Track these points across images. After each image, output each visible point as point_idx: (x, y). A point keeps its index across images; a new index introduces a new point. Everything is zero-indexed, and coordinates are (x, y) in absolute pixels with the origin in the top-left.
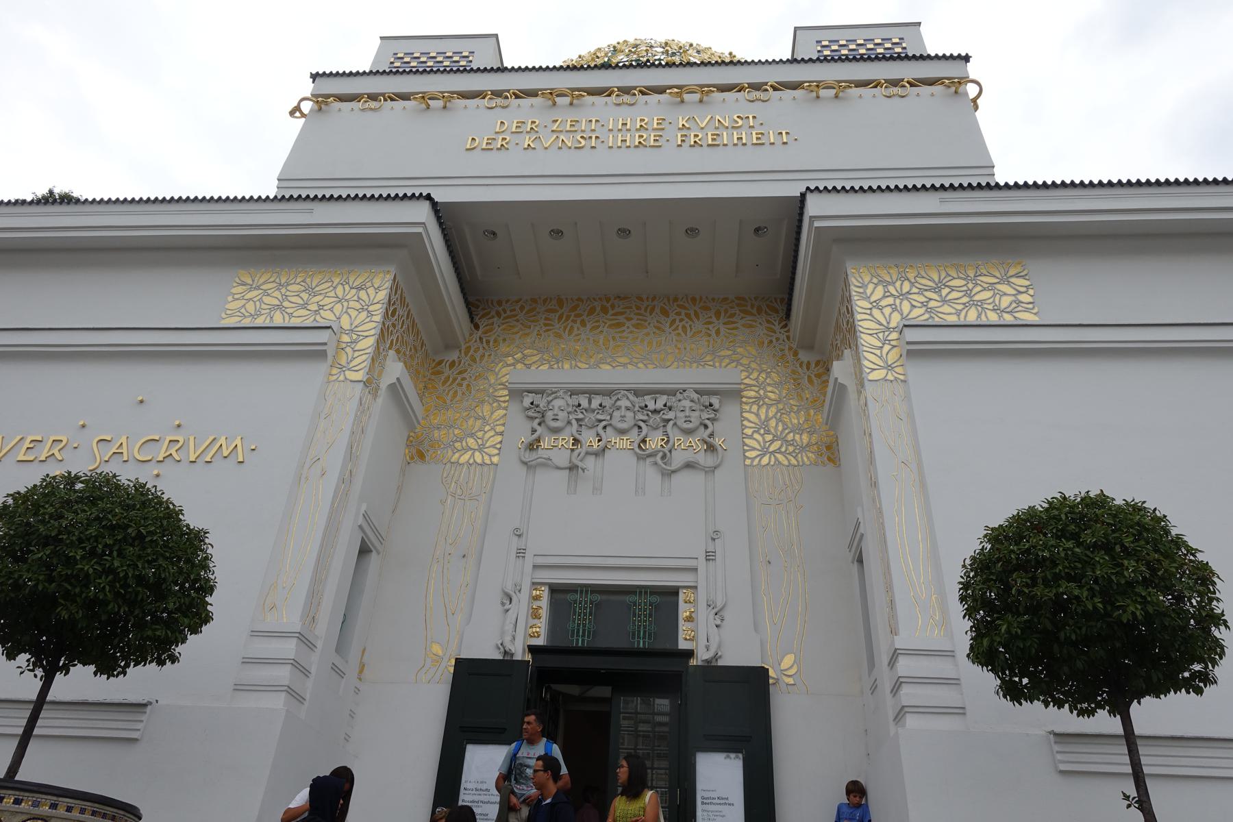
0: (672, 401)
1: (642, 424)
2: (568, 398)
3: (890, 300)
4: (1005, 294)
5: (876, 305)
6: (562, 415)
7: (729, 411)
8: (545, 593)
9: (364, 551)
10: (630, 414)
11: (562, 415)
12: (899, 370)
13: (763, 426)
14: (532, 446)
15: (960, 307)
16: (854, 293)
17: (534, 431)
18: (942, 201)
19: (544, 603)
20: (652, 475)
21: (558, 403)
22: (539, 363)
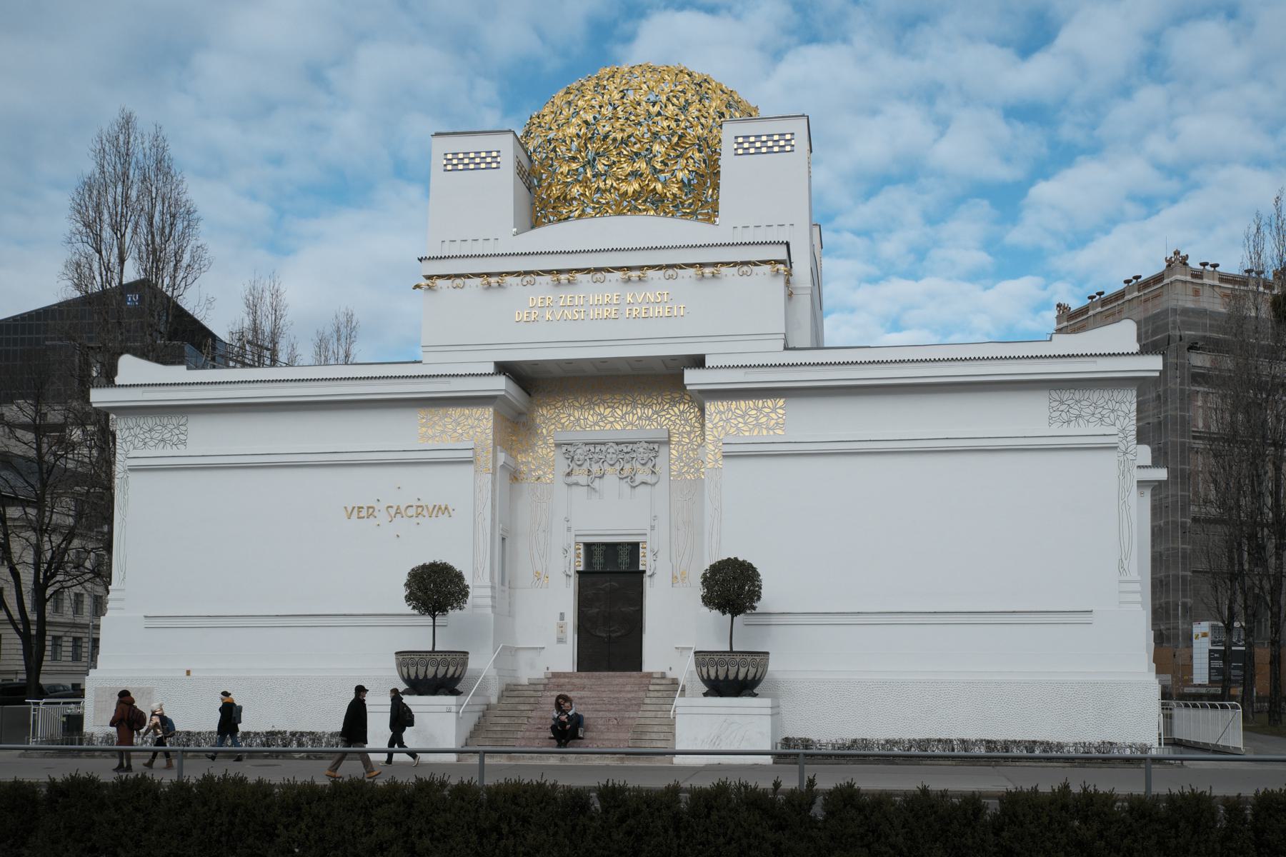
0: (635, 446)
1: (621, 460)
2: (583, 446)
3: (721, 423)
4: (773, 419)
5: (715, 426)
6: (582, 457)
7: (663, 450)
8: (582, 546)
9: (503, 539)
10: (615, 456)
11: (582, 457)
12: (720, 462)
13: (680, 458)
14: (569, 474)
15: (751, 427)
16: (706, 419)
17: (569, 466)
18: (746, 373)
19: (582, 551)
20: (625, 486)
21: (579, 451)
22: (567, 423)
